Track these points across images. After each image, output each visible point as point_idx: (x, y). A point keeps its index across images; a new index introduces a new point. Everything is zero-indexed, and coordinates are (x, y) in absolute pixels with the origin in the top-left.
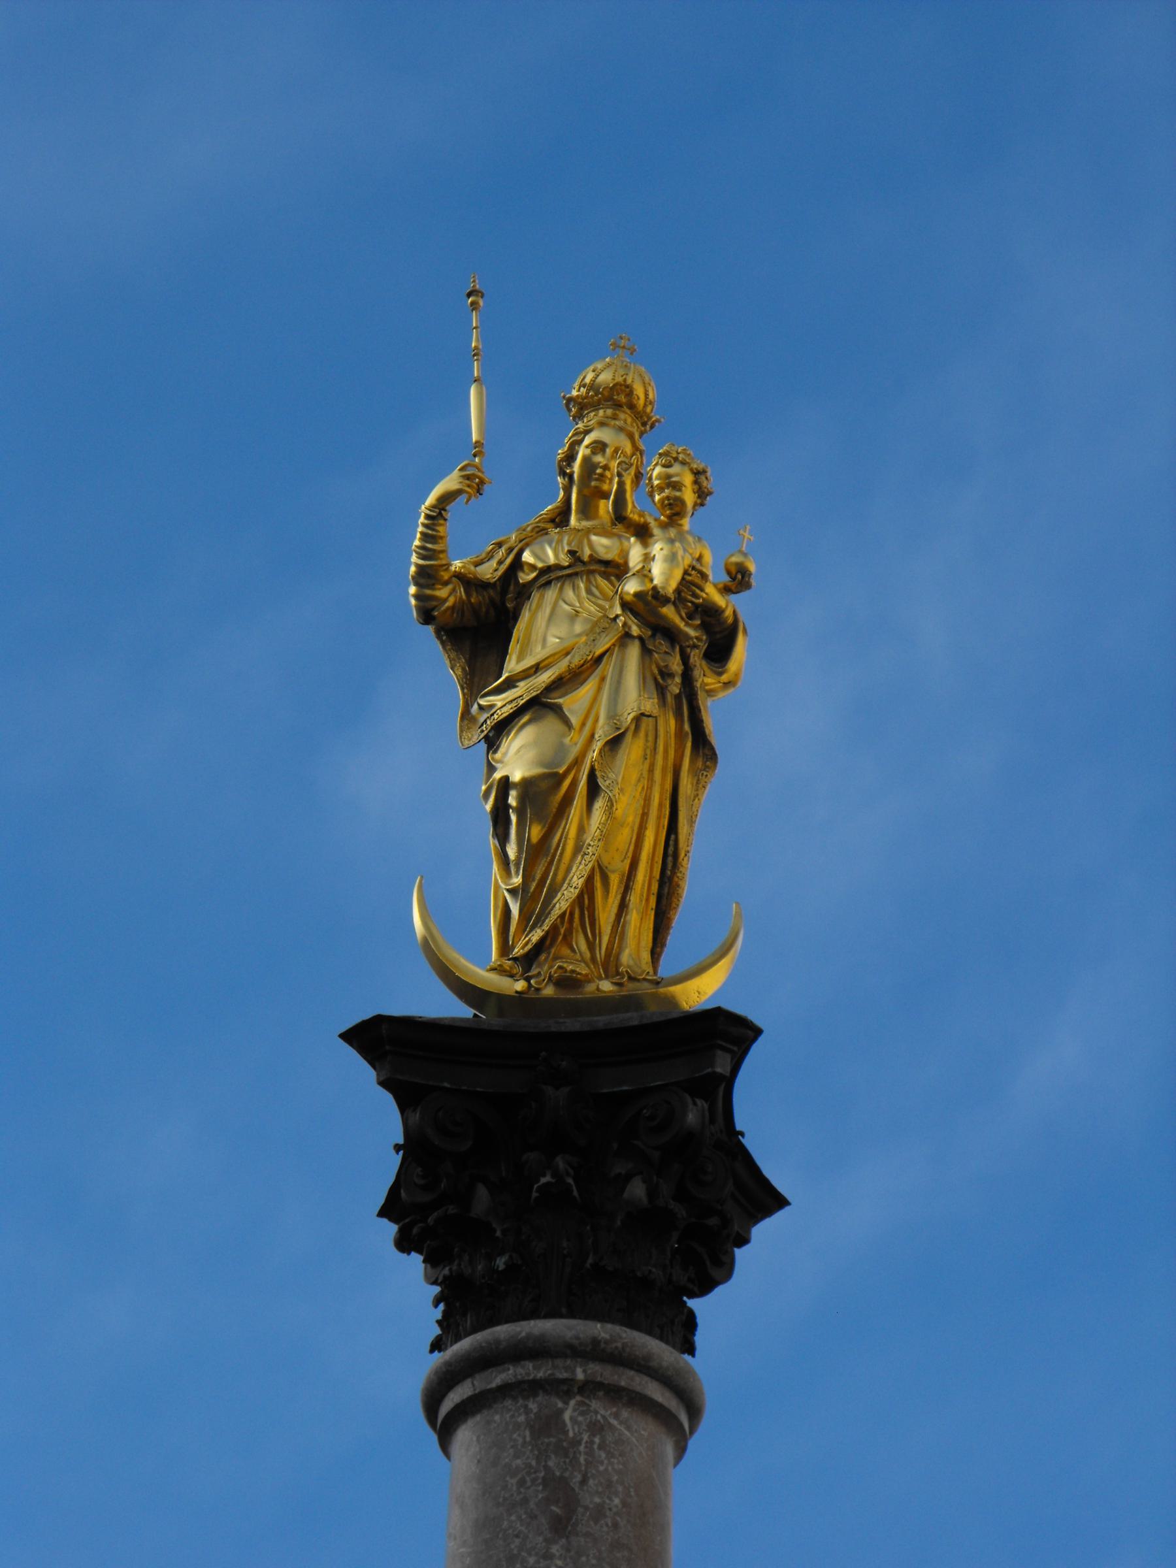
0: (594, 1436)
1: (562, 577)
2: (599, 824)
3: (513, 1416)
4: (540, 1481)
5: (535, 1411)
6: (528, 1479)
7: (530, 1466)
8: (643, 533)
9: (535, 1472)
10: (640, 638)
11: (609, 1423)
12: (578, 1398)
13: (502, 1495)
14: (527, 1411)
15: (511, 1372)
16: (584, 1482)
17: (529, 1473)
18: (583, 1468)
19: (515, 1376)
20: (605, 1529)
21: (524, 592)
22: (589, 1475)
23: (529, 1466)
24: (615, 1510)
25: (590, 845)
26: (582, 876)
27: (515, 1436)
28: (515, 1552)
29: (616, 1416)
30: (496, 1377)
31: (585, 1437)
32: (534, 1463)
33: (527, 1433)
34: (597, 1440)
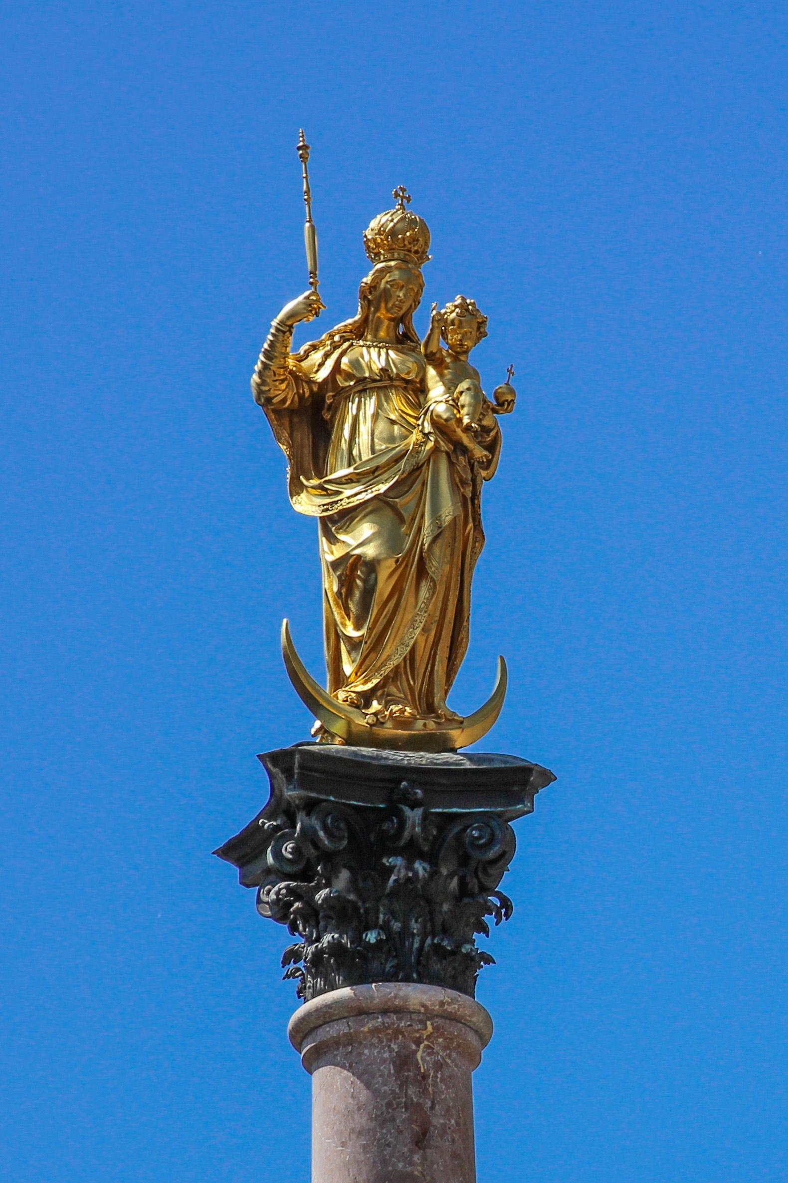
1: (374, 388)
2: (424, 599)
3: (379, 1052)
4: (403, 1105)
5: (396, 1050)
6: (394, 1102)
9: (399, 1098)
10: (447, 453)
11: (446, 1062)
12: (426, 1043)
13: (374, 1112)
14: (391, 1050)
15: (380, 1020)
16: (432, 1107)
17: (394, 1098)
18: (432, 1097)
19: (383, 1023)
20: (447, 1143)
21: (343, 395)
22: (436, 1102)
23: (393, 1092)
24: (452, 1128)
25: (418, 614)
26: (412, 638)
28: (388, 1157)
29: (449, 1056)
30: (368, 1022)
32: (397, 1090)
33: (392, 1067)
34: (439, 1076)
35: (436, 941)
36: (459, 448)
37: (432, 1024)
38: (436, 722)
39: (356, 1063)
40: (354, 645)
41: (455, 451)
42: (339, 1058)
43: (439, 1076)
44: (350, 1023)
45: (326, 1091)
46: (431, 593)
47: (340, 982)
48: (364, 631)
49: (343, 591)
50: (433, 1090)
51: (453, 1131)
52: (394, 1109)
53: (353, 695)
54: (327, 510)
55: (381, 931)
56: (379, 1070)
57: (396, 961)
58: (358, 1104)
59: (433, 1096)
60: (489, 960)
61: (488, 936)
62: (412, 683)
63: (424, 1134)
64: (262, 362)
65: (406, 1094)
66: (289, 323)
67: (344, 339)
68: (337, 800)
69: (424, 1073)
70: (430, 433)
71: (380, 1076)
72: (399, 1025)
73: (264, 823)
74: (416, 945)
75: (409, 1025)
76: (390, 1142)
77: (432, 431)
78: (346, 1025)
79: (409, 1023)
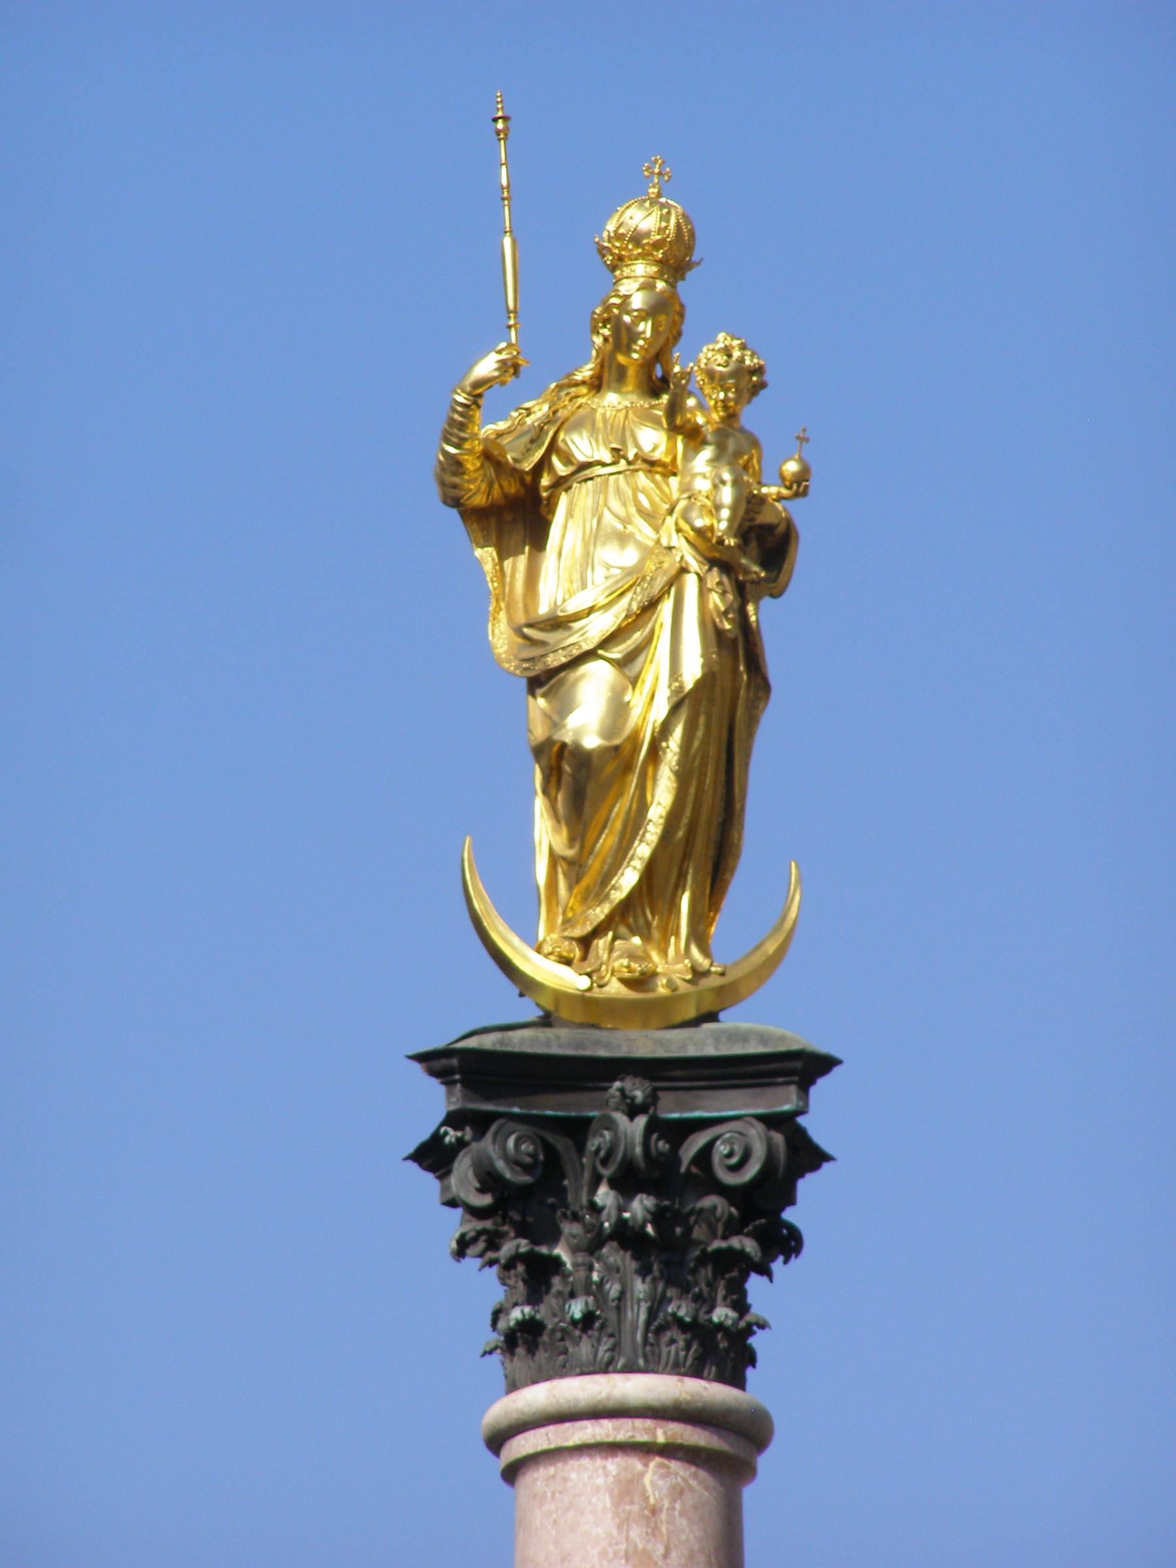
0: (675, 1501)
3: (590, 1477)
8: (694, 436)
9: (617, 1544)
17: (610, 1545)
22: (672, 1546)
27: (594, 1500)
31: (666, 1504)
32: (615, 1532)
34: (678, 1506)
39: (560, 1493)
44: (550, 1435)
50: (667, 1529)
56: (590, 1503)
57: (612, 1341)
59: (668, 1538)
60: (762, 1326)
61: (771, 1281)
65: (627, 1538)
68: (524, 1111)
69: (654, 1505)
71: (591, 1512)
78: (545, 1438)
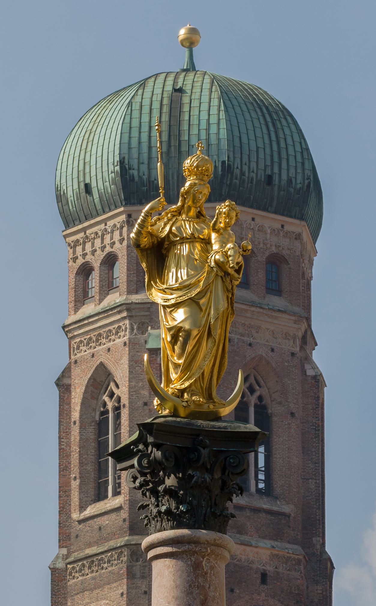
4: (196, 586)
5: (194, 561)
7: (193, 581)
10: (221, 277)
12: (207, 557)
15: (187, 547)
16: (209, 588)
17: (193, 583)
20: (215, 604)
21: (173, 244)
24: (217, 597)
30: (181, 547)
32: (194, 579)
33: (192, 568)
35: (212, 510)
36: (227, 274)
37: (210, 549)
38: (213, 405)
40: (176, 366)
41: (225, 276)
42: (167, 562)
43: (212, 572)
45: (160, 576)
46: (213, 344)
47: (169, 527)
48: (181, 361)
49: (173, 341)
51: (218, 598)
52: (192, 588)
53: (176, 391)
54: (166, 302)
55: (188, 505)
58: (176, 584)
62: (202, 385)
63: (206, 600)
64: (137, 228)
66: (150, 212)
67: (174, 216)
70: (214, 267)
72: (195, 550)
73: (133, 448)
74: (204, 512)
75: (201, 550)
76: (190, 604)
77: (215, 266)
79: (200, 549)
